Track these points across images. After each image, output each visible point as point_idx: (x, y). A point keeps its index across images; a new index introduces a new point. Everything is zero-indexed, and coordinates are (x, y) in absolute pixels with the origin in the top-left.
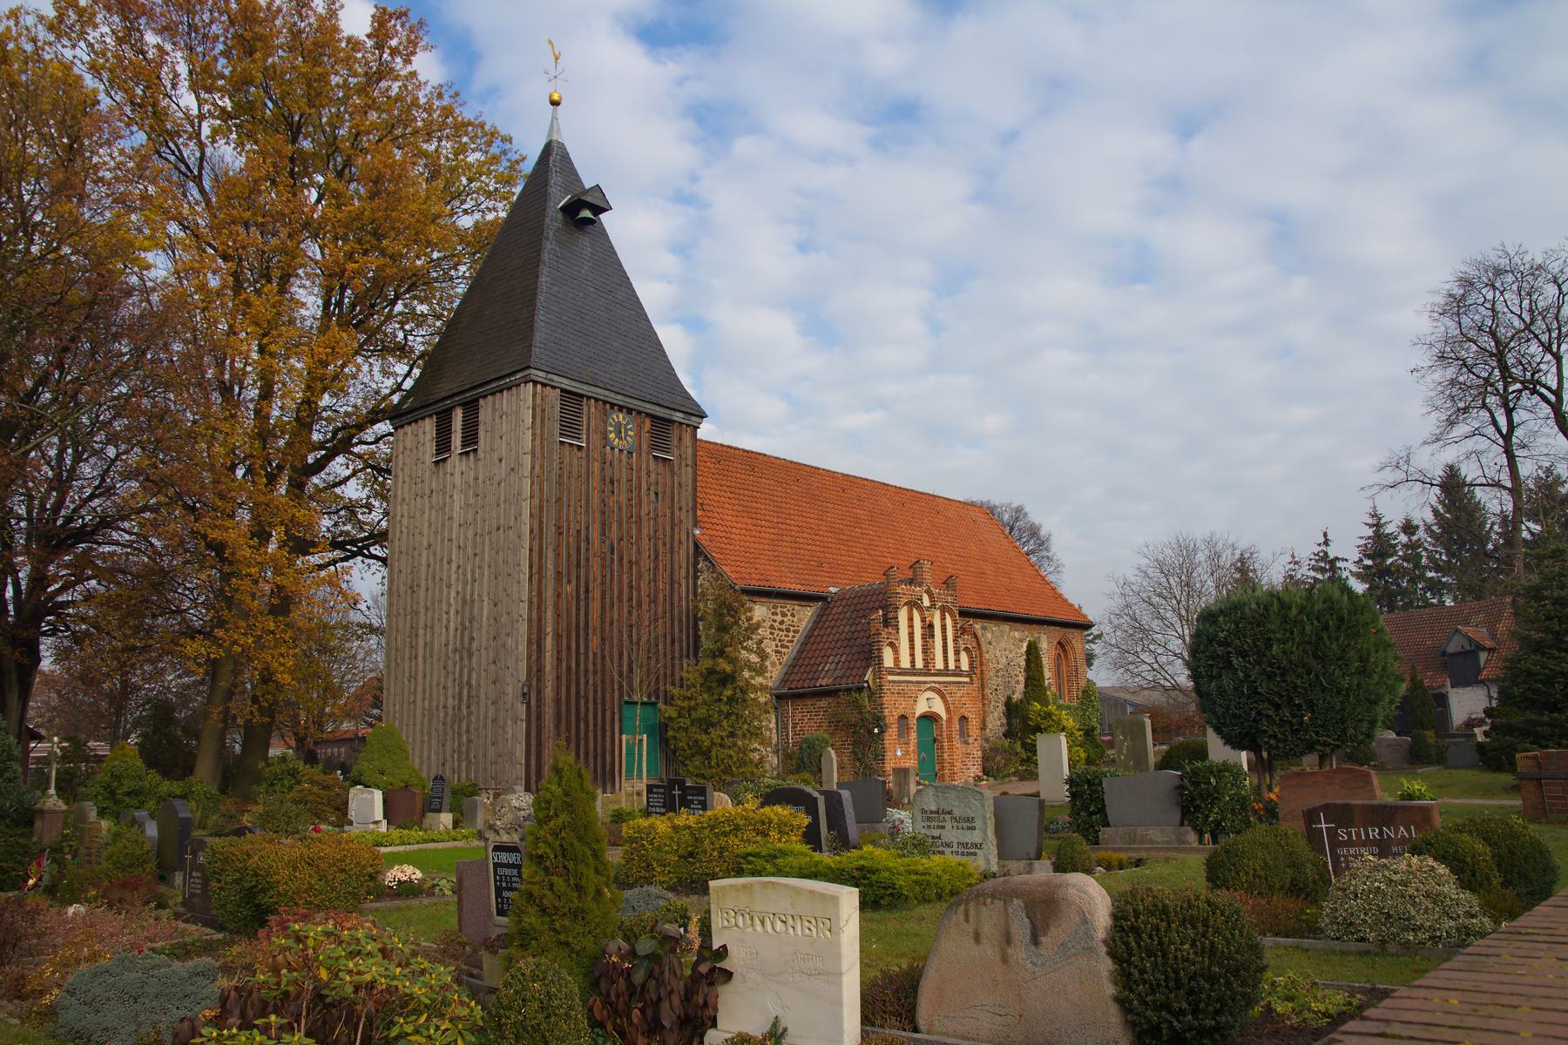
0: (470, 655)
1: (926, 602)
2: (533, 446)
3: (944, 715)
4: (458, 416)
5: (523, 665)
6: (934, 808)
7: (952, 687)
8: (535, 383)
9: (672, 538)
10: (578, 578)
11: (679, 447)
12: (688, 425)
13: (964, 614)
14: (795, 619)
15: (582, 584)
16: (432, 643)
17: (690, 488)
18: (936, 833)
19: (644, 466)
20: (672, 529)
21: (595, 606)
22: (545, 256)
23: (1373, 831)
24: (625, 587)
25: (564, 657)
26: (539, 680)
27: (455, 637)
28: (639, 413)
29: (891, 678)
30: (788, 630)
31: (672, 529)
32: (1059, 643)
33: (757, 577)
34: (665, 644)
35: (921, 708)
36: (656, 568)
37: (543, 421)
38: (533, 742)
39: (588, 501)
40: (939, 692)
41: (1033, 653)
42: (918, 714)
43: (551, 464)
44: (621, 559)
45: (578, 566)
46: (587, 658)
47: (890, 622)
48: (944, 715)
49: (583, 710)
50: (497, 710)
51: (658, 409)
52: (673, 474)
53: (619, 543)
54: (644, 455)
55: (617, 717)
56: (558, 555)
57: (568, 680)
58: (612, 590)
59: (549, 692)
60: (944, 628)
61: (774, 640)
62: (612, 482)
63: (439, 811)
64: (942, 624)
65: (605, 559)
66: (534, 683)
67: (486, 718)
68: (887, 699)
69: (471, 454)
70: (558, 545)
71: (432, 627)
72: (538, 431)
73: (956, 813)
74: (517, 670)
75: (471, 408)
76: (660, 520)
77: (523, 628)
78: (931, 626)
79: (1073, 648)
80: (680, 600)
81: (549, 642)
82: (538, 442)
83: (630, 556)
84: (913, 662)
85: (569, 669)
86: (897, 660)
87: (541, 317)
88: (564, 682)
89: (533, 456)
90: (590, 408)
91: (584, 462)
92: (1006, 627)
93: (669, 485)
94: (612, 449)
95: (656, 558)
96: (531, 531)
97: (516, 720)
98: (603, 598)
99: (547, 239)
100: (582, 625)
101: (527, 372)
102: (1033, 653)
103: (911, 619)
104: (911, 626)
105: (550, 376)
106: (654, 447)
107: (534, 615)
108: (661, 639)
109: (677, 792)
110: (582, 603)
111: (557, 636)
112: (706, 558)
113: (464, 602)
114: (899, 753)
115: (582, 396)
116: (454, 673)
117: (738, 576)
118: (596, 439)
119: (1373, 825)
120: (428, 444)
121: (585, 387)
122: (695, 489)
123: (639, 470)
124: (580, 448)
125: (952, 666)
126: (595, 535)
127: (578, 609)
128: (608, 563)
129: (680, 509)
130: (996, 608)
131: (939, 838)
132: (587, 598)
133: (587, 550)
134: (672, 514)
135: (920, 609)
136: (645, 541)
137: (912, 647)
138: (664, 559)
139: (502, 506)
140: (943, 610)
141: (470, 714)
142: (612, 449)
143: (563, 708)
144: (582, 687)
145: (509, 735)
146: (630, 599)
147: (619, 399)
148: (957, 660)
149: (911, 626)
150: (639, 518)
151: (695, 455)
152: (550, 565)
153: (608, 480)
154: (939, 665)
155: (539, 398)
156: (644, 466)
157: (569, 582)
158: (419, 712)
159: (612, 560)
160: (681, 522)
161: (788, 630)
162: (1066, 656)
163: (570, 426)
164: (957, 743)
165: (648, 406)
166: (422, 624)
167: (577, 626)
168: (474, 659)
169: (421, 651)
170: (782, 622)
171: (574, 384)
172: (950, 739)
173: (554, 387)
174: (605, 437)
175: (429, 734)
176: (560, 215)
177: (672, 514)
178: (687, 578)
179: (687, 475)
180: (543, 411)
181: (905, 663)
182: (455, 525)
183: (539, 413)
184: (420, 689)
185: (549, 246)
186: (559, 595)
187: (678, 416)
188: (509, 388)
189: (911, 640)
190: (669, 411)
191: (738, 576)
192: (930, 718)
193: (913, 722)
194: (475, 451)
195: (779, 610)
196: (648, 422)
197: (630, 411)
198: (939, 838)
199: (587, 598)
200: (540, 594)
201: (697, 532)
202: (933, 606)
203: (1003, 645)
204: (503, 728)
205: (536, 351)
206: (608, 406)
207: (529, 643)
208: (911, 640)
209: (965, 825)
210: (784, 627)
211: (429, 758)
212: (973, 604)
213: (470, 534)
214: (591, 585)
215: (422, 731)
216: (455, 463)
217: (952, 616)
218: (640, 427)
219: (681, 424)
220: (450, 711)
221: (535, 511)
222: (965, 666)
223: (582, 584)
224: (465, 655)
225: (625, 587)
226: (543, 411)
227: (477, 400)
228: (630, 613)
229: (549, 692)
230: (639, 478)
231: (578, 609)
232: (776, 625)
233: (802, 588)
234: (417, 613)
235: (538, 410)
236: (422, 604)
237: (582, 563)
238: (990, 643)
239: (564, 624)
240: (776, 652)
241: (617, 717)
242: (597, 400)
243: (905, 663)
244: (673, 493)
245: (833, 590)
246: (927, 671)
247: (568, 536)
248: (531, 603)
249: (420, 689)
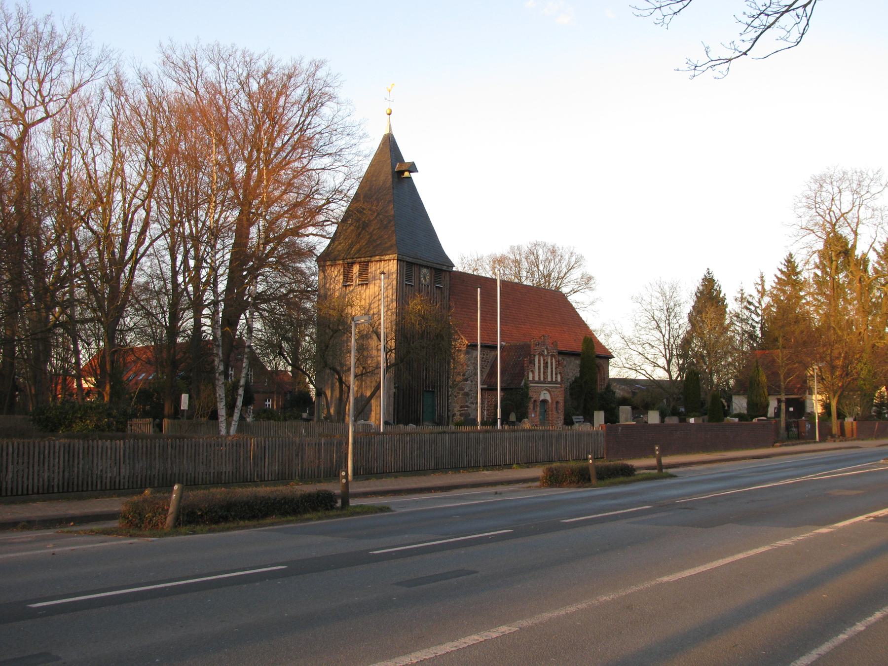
1: (546, 353)
3: (550, 401)
7: (554, 389)
28: (431, 268)
29: (531, 385)
35: (542, 398)
42: (541, 399)
47: (532, 362)
48: (550, 401)
64: (552, 362)
78: (547, 363)
84: (539, 378)
86: (534, 377)
92: (573, 359)
103: (539, 360)
106: (435, 282)
125: (554, 380)
137: (539, 372)
140: (552, 356)
148: (556, 377)
154: (549, 379)
174: (420, 280)
181: (537, 379)
189: (539, 369)
192: (544, 402)
193: (538, 403)
208: (539, 369)
222: (559, 380)
233: (492, 343)
243: (537, 379)
246: (544, 382)
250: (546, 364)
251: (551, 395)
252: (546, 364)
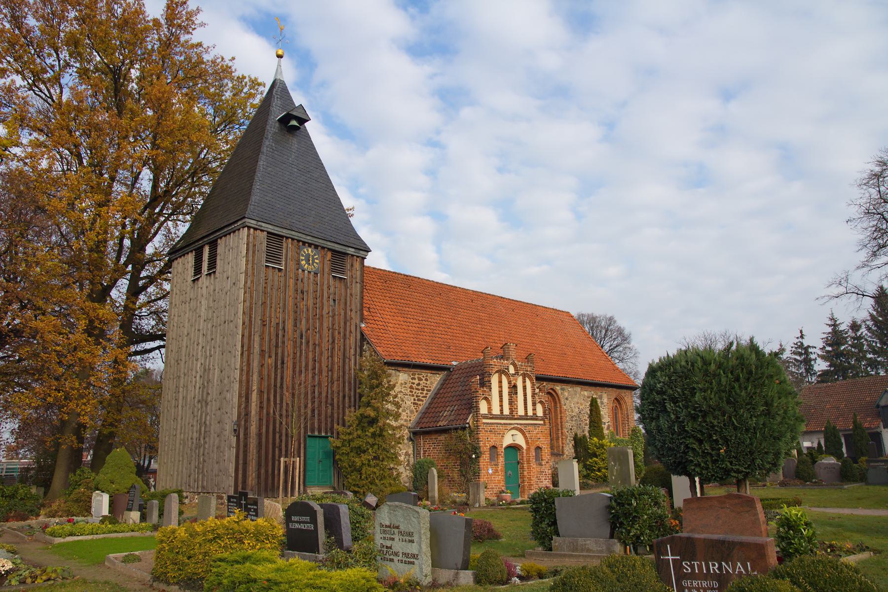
0: (207, 404)
1: (512, 370)
2: (247, 268)
4: (206, 250)
5: (235, 411)
6: (388, 523)
7: (530, 428)
8: (249, 228)
9: (345, 329)
10: (276, 354)
11: (351, 270)
12: (358, 257)
13: (539, 379)
14: (428, 382)
15: (279, 358)
16: (186, 397)
17: (358, 297)
18: (389, 543)
19: (326, 282)
20: (345, 323)
21: (288, 373)
22: (264, 149)
23: (714, 565)
24: (311, 360)
25: (265, 406)
26: (246, 421)
27: (199, 392)
28: (323, 248)
29: (485, 421)
30: (423, 389)
31: (345, 323)
32: (616, 399)
33: (401, 355)
34: (338, 398)
35: (508, 441)
36: (333, 348)
37: (254, 252)
38: (241, 462)
39: (285, 304)
40: (521, 431)
41: (594, 407)
42: (505, 445)
43: (259, 280)
44: (308, 343)
45: (277, 346)
46: (281, 407)
47: (485, 383)
49: (277, 441)
50: (220, 441)
51: (336, 245)
52: (346, 287)
53: (306, 332)
54: (326, 275)
55: (302, 446)
56: (262, 339)
57: (268, 421)
58: (300, 362)
59: (253, 429)
60: (525, 388)
61: (413, 396)
62: (302, 292)
63: (130, 510)
64: (526, 387)
65: (296, 342)
66: (243, 423)
67: (214, 446)
68: (482, 435)
69: (212, 275)
70: (263, 333)
71: (187, 387)
72: (251, 258)
73: (402, 528)
74: (232, 414)
75: (213, 245)
76: (336, 317)
77: (236, 386)
78: (515, 386)
79: (625, 402)
80: (350, 369)
81: (254, 396)
82: (250, 266)
83: (314, 340)
84: (502, 410)
85: (268, 414)
86: (490, 409)
87: (257, 186)
88: (264, 422)
89: (246, 274)
90: (288, 245)
91: (282, 279)
93: (343, 294)
94: (303, 271)
95: (333, 342)
96: (244, 324)
97: (230, 447)
98: (294, 368)
99: (267, 138)
100: (278, 385)
101: (243, 221)
102: (594, 407)
103: (500, 382)
104: (501, 387)
105: (260, 223)
107: (244, 378)
108: (335, 395)
109: (243, 502)
110: (279, 371)
111: (261, 392)
112: (368, 343)
113: (205, 370)
114: (490, 471)
115: (282, 237)
116: (197, 416)
117: (387, 354)
118: (292, 265)
119: (713, 559)
120: (190, 269)
121: (284, 231)
122: (362, 298)
123: (322, 285)
124: (280, 270)
125: (530, 413)
126: (289, 325)
127: (276, 375)
128: (298, 344)
129: (351, 310)
130: (570, 376)
131: (390, 548)
132: (282, 367)
133: (284, 336)
134: (345, 313)
135: (507, 375)
136: (325, 331)
137: (501, 401)
138: (339, 343)
139: (227, 307)
140: (524, 376)
141: (205, 443)
142: (303, 271)
143: (264, 440)
144: (278, 425)
145: (226, 457)
146: (314, 368)
147: (308, 239)
148: (534, 410)
149: (501, 387)
150: (322, 316)
151: (362, 276)
153: (299, 291)
154: (521, 412)
155: (251, 237)
156: (326, 282)
157: (270, 357)
158: (178, 441)
159: (301, 343)
160: (351, 318)
161: (423, 389)
162: (621, 409)
163: (273, 255)
164: (533, 465)
165: (329, 243)
166: (182, 385)
167: (275, 386)
168: (209, 407)
169: (180, 402)
170: (418, 384)
171: (276, 228)
172: (528, 462)
173: (262, 231)
174: (298, 263)
175: (183, 456)
176: (277, 125)
177: (345, 313)
178: (355, 355)
179: (357, 289)
180: (254, 246)
181: (496, 411)
182: (202, 321)
183: (251, 248)
184: (179, 427)
185: (267, 143)
186: (262, 365)
187: (351, 251)
188: (234, 232)
190: (344, 247)
191: (387, 354)
192: (514, 448)
193: (501, 451)
194: (214, 272)
195: (416, 376)
196: (329, 254)
197: (316, 247)
198: (390, 548)
199: (282, 367)
200: (249, 364)
201: (363, 325)
202: (517, 373)
203: (575, 400)
204: (223, 452)
205: (251, 207)
206: (301, 243)
207: (240, 396)
209: (408, 538)
210: (420, 387)
211: (182, 472)
212: (553, 372)
213: (210, 326)
214: (286, 359)
215: (179, 454)
216: (204, 281)
217: (531, 380)
218: (323, 257)
219: (353, 256)
220: (194, 441)
221: (247, 311)
222: (540, 412)
223: (279, 358)
224: (204, 404)
225: (311, 360)
226: (254, 246)
227: (216, 240)
228: (313, 377)
229: (253, 429)
230: (322, 290)
231: (276, 375)
232: (414, 386)
233: (432, 362)
234: (179, 377)
235: (251, 245)
236: (182, 372)
237: (280, 344)
238: (567, 399)
239: (265, 384)
240: (414, 404)
241: (302, 446)
242: (293, 239)
243: (496, 411)
244: (346, 300)
245: (454, 363)
246: (512, 416)
247: (270, 327)
248: (242, 370)
249: (179, 427)
250: (513, 388)
251: (525, 437)
252: (513, 388)
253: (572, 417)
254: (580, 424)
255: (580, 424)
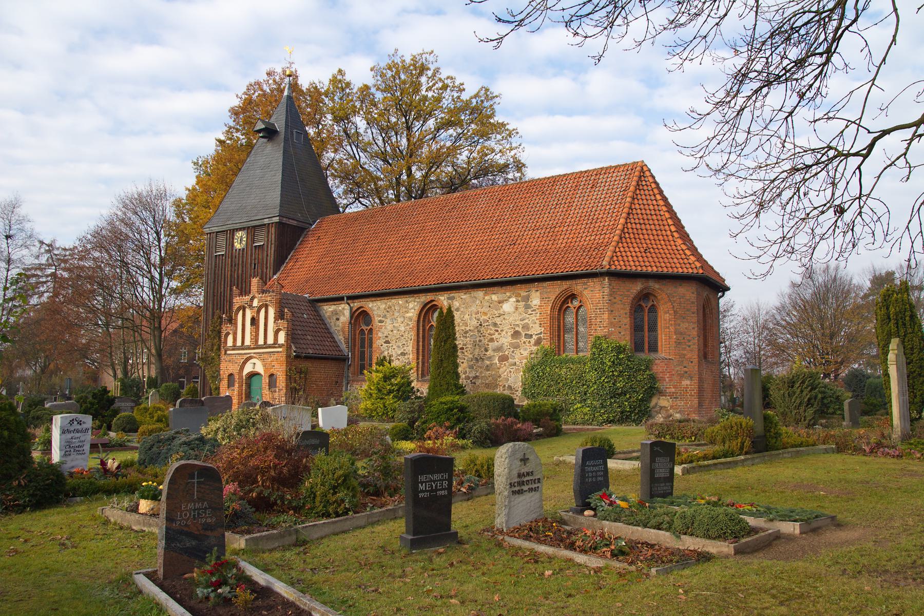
28: (249, 227)
35: (248, 369)
124: (223, 255)
152: (211, 310)
154: (261, 342)
187: (266, 221)
219: (269, 224)
243: (239, 343)
253: (466, 332)
254: (480, 341)
255: (480, 341)
